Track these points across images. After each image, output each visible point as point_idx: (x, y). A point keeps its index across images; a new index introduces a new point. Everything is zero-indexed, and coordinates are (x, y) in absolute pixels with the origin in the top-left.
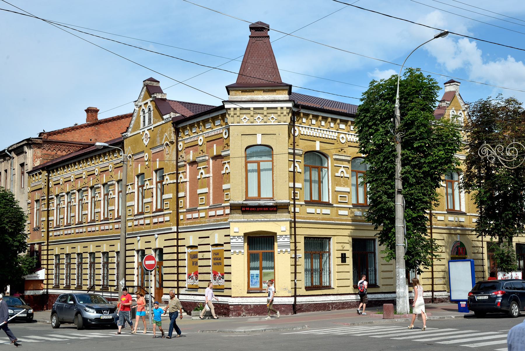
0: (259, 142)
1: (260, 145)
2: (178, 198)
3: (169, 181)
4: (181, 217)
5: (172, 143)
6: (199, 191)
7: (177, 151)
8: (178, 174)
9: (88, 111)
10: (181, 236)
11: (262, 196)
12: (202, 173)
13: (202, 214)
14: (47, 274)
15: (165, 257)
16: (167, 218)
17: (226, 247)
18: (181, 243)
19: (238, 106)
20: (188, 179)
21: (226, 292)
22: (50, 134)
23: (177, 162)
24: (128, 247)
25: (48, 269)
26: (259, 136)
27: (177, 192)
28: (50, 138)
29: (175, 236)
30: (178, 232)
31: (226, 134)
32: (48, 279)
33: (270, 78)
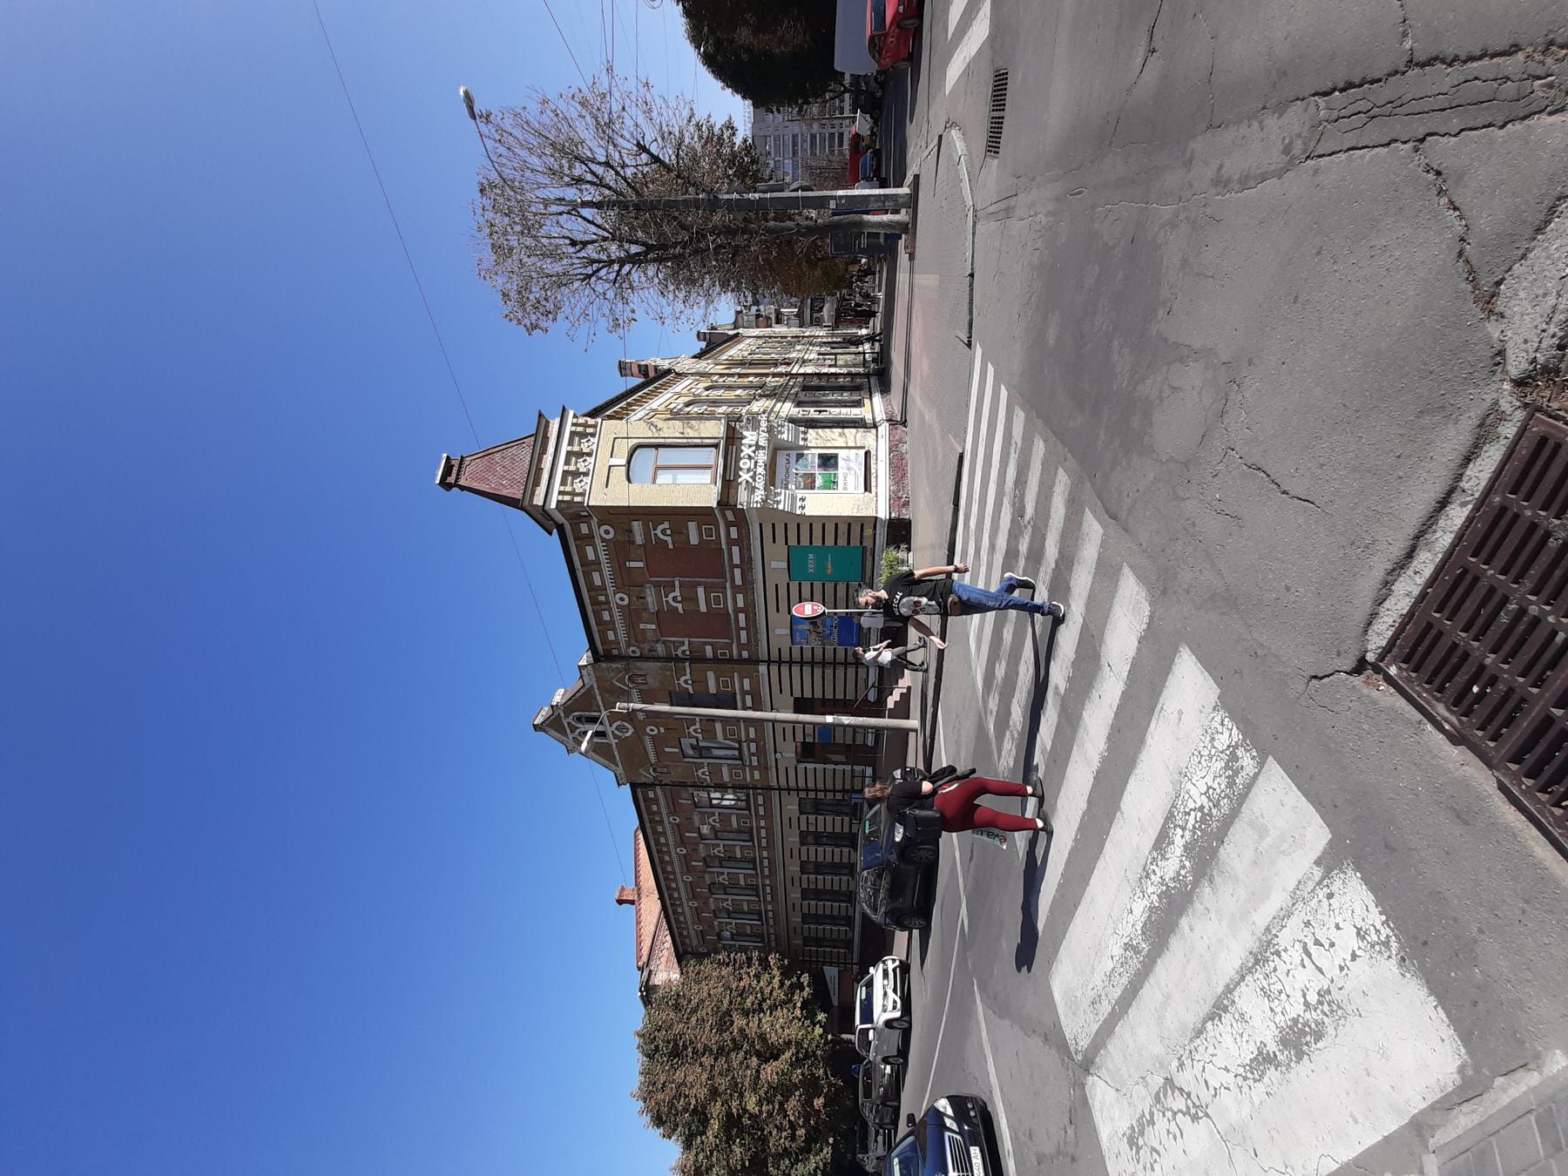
0: (624, 462)
1: (629, 462)
2: (715, 660)
3: (688, 677)
4: (745, 654)
5: (627, 670)
6: (703, 608)
7: (642, 658)
8: (677, 659)
9: (620, 902)
10: (774, 656)
11: (711, 462)
12: (674, 599)
13: (740, 597)
14: (831, 964)
15: (808, 695)
16: (746, 682)
17: (793, 541)
18: (785, 656)
19: (557, 486)
20: (686, 641)
21: (868, 543)
22: (639, 958)
23: (657, 659)
24: (792, 784)
25: (824, 963)
26: (614, 461)
27: (704, 660)
28: (645, 958)
29: (774, 668)
30: (769, 662)
31: (607, 532)
32: (838, 964)
33: (524, 454)
